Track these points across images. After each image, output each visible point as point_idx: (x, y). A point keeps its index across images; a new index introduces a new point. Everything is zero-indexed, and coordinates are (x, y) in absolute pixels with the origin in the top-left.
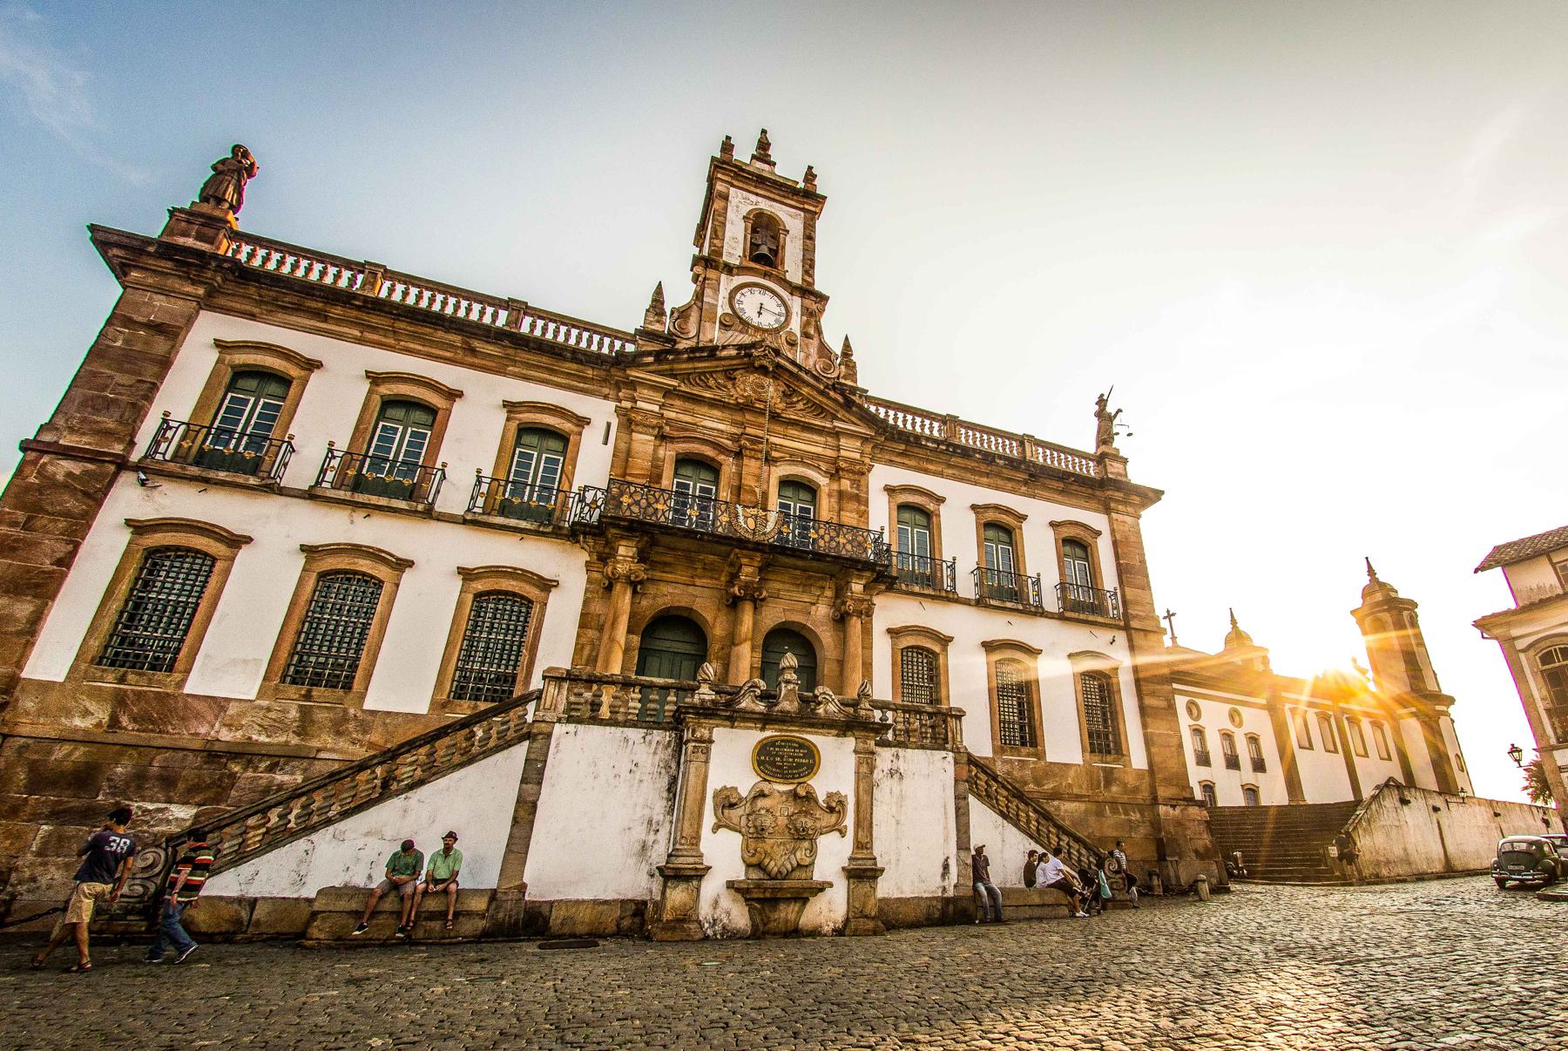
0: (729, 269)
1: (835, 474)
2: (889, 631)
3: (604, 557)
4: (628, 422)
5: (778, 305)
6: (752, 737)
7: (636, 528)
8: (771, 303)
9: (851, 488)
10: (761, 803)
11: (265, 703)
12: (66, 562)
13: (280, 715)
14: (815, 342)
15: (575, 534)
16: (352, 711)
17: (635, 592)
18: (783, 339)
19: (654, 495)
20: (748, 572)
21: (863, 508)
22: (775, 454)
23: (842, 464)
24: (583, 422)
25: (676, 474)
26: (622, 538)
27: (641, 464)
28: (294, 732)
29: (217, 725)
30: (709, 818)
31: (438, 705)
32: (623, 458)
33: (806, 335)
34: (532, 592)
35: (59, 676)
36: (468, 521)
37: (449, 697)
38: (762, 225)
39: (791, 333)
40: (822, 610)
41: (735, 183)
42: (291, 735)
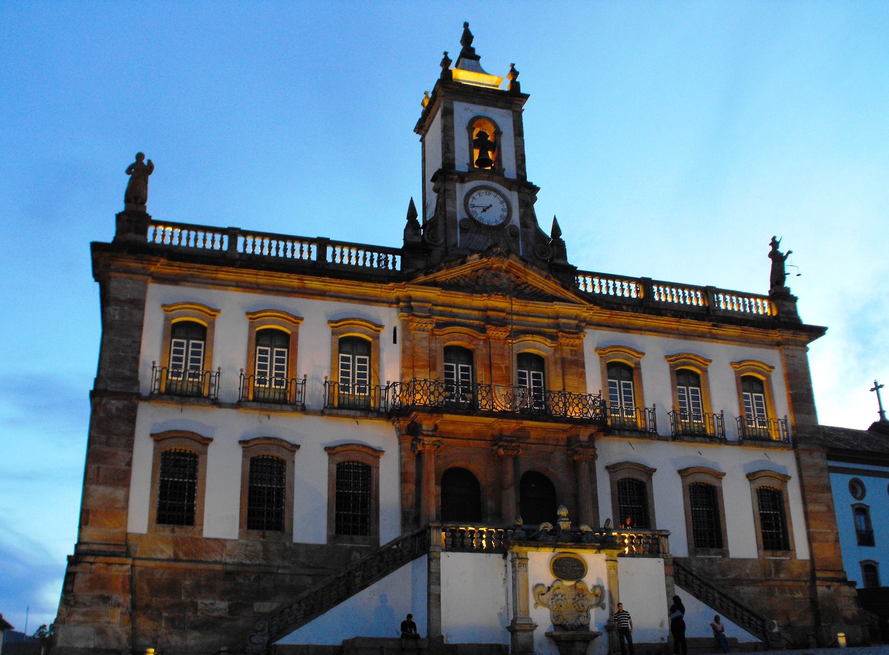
0: (463, 178)
2: (607, 468)
5: (501, 203)
9: (572, 355)
11: (244, 541)
12: (129, 464)
13: (253, 548)
14: (533, 227)
16: (288, 544)
18: (508, 233)
19: (442, 387)
26: (425, 419)
28: (262, 558)
29: (224, 555)
31: (329, 538)
33: (524, 224)
35: (144, 531)
37: (336, 532)
39: (513, 227)
42: (261, 560)
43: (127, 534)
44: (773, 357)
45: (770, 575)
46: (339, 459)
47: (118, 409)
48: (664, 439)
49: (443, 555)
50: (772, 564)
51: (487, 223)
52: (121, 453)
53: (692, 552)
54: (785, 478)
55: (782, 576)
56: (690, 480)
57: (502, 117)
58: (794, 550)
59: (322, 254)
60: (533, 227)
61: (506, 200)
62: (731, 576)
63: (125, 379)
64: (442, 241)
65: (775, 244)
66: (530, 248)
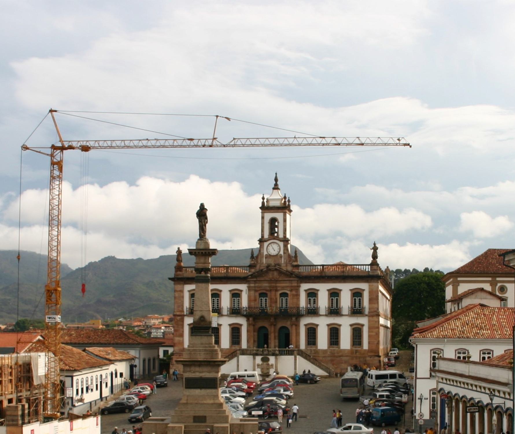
0: (266, 241)
1: (291, 291)
3: (248, 320)
4: (249, 289)
5: (278, 247)
8: (275, 247)
10: (262, 365)
12: (183, 332)
14: (287, 253)
17: (254, 325)
20: (272, 320)
21: (298, 297)
22: (278, 288)
23: (292, 288)
24: (241, 291)
25: (260, 297)
27: (253, 298)
30: (256, 367)
31: (231, 346)
33: (284, 253)
36: (227, 315)
38: (273, 221)
39: (281, 254)
41: (265, 211)
44: (364, 286)
45: (353, 353)
46: (232, 327)
47: (180, 319)
48: (323, 315)
50: (355, 351)
51: (272, 254)
53: (329, 347)
55: (357, 354)
57: (279, 216)
58: (363, 346)
59: (227, 271)
60: (287, 253)
61: (279, 246)
62: (340, 354)
64: (259, 262)
65: (375, 244)
66: (285, 261)
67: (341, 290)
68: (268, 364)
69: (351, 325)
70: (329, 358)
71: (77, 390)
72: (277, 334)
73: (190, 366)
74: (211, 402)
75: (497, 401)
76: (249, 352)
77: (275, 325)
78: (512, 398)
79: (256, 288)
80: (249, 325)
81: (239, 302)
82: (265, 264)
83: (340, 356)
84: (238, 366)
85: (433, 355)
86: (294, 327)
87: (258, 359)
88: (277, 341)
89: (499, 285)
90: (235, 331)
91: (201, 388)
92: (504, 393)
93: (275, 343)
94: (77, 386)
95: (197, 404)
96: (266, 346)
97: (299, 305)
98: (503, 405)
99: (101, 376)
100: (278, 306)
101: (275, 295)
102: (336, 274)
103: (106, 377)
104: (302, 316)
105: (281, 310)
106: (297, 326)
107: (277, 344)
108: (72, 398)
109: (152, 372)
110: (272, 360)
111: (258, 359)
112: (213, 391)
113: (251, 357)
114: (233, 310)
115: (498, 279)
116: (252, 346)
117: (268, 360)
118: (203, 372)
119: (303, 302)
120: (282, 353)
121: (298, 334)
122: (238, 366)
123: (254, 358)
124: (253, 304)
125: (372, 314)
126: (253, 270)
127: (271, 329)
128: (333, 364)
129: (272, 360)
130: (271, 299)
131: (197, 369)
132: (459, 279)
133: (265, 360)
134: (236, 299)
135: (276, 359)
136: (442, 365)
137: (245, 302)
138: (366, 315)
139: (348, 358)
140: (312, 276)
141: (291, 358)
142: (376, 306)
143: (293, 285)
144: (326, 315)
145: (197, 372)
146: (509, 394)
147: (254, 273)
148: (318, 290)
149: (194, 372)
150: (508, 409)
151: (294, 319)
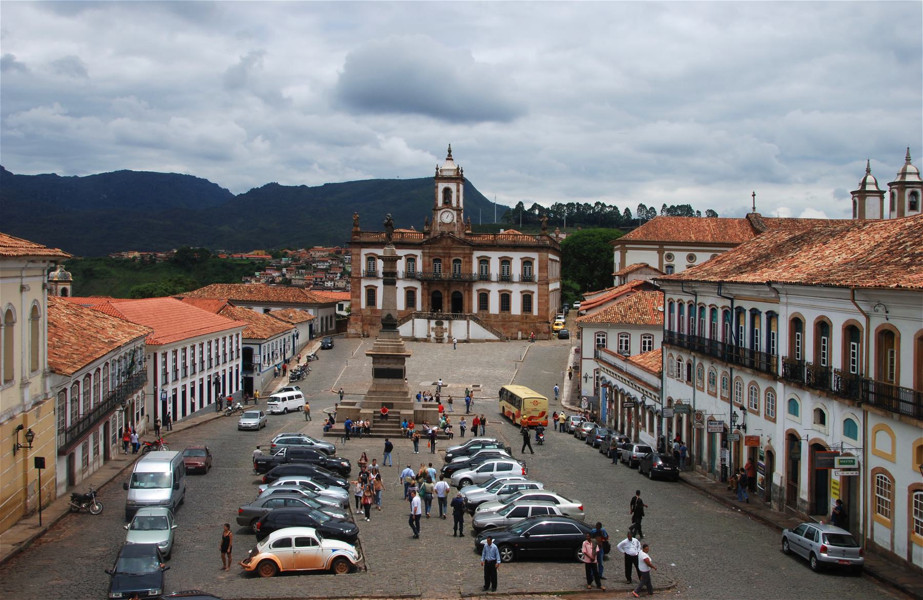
0: (440, 210)
1: (464, 258)
3: (422, 284)
4: (424, 254)
6: (434, 321)
7: (426, 280)
15: (418, 280)
17: (428, 290)
20: (446, 285)
24: (416, 256)
27: (427, 263)
31: (406, 309)
32: (424, 262)
33: (457, 221)
34: (414, 290)
40: (462, 288)
43: (361, 309)
44: (534, 255)
46: (407, 290)
48: (494, 282)
49: (415, 319)
52: (358, 291)
54: (533, 292)
55: (528, 320)
56: (502, 293)
59: (403, 236)
62: (511, 319)
63: (358, 274)
67: (512, 259)
68: (442, 328)
69: (521, 292)
70: (500, 323)
71: (264, 356)
72: (450, 298)
73: (379, 358)
74: (398, 390)
75: (649, 402)
76: (423, 316)
77: (448, 291)
78: (661, 402)
79: (431, 254)
80: (423, 289)
81: (414, 267)
82: (440, 231)
83: (511, 321)
84: (413, 328)
85: (597, 337)
86: (466, 292)
87: (433, 323)
88: (450, 305)
89: (666, 252)
90: (410, 295)
91: (388, 378)
92: (655, 396)
93: (448, 306)
94: (264, 353)
95: (385, 391)
96: (440, 310)
97: (472, 271)
98: (654, 407)
99: (285, 339)
100: (452, 272)
101: (449, 262)
102: (507, 243)
103: (289, 340)
104: (475, 281)
105: (454, 275)
106: (470, 291)
107: (450, 308)
108: (260, 364)
109: (329, 329)
110: (446, 324)
111: (433, 323)
112: (400, 380)
113: (427, 320)
114: (408, 274)
115: (665, 247)
116: (426, 310)
117: (442, 324)
118: (389, 364)
119: (475, 269)
120: (456, 317)
121: (470, 299)
122: (413, 328)
123: (429, 322)
124: (427, 269)
125: (541, 282)
126: (427, 237)
127: (445, 294)
128: (504, 329)
129: (446, 324)
130: (445, 265)
131: (385, 361)
132: (627, 246)
133: (439, 323)
134: (411, 264)
135: (450, 323)
136: (603, 355)
137: (419, 267)
138: (536, 283)
139: (518, 323)
140: (485, 244)
141: (463, 323)
142: (545, 274)
143: (466, 252)
144: (497, 282)
145: (385, 363)
146: (659, 399)
147: (428, 240)
148: (490, 258)
149: (383, 364)
150: (657, 411)
151: (467, 284)
